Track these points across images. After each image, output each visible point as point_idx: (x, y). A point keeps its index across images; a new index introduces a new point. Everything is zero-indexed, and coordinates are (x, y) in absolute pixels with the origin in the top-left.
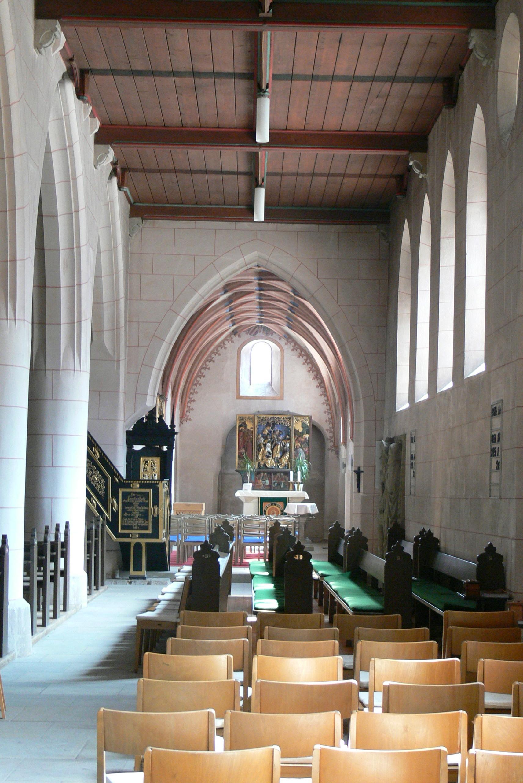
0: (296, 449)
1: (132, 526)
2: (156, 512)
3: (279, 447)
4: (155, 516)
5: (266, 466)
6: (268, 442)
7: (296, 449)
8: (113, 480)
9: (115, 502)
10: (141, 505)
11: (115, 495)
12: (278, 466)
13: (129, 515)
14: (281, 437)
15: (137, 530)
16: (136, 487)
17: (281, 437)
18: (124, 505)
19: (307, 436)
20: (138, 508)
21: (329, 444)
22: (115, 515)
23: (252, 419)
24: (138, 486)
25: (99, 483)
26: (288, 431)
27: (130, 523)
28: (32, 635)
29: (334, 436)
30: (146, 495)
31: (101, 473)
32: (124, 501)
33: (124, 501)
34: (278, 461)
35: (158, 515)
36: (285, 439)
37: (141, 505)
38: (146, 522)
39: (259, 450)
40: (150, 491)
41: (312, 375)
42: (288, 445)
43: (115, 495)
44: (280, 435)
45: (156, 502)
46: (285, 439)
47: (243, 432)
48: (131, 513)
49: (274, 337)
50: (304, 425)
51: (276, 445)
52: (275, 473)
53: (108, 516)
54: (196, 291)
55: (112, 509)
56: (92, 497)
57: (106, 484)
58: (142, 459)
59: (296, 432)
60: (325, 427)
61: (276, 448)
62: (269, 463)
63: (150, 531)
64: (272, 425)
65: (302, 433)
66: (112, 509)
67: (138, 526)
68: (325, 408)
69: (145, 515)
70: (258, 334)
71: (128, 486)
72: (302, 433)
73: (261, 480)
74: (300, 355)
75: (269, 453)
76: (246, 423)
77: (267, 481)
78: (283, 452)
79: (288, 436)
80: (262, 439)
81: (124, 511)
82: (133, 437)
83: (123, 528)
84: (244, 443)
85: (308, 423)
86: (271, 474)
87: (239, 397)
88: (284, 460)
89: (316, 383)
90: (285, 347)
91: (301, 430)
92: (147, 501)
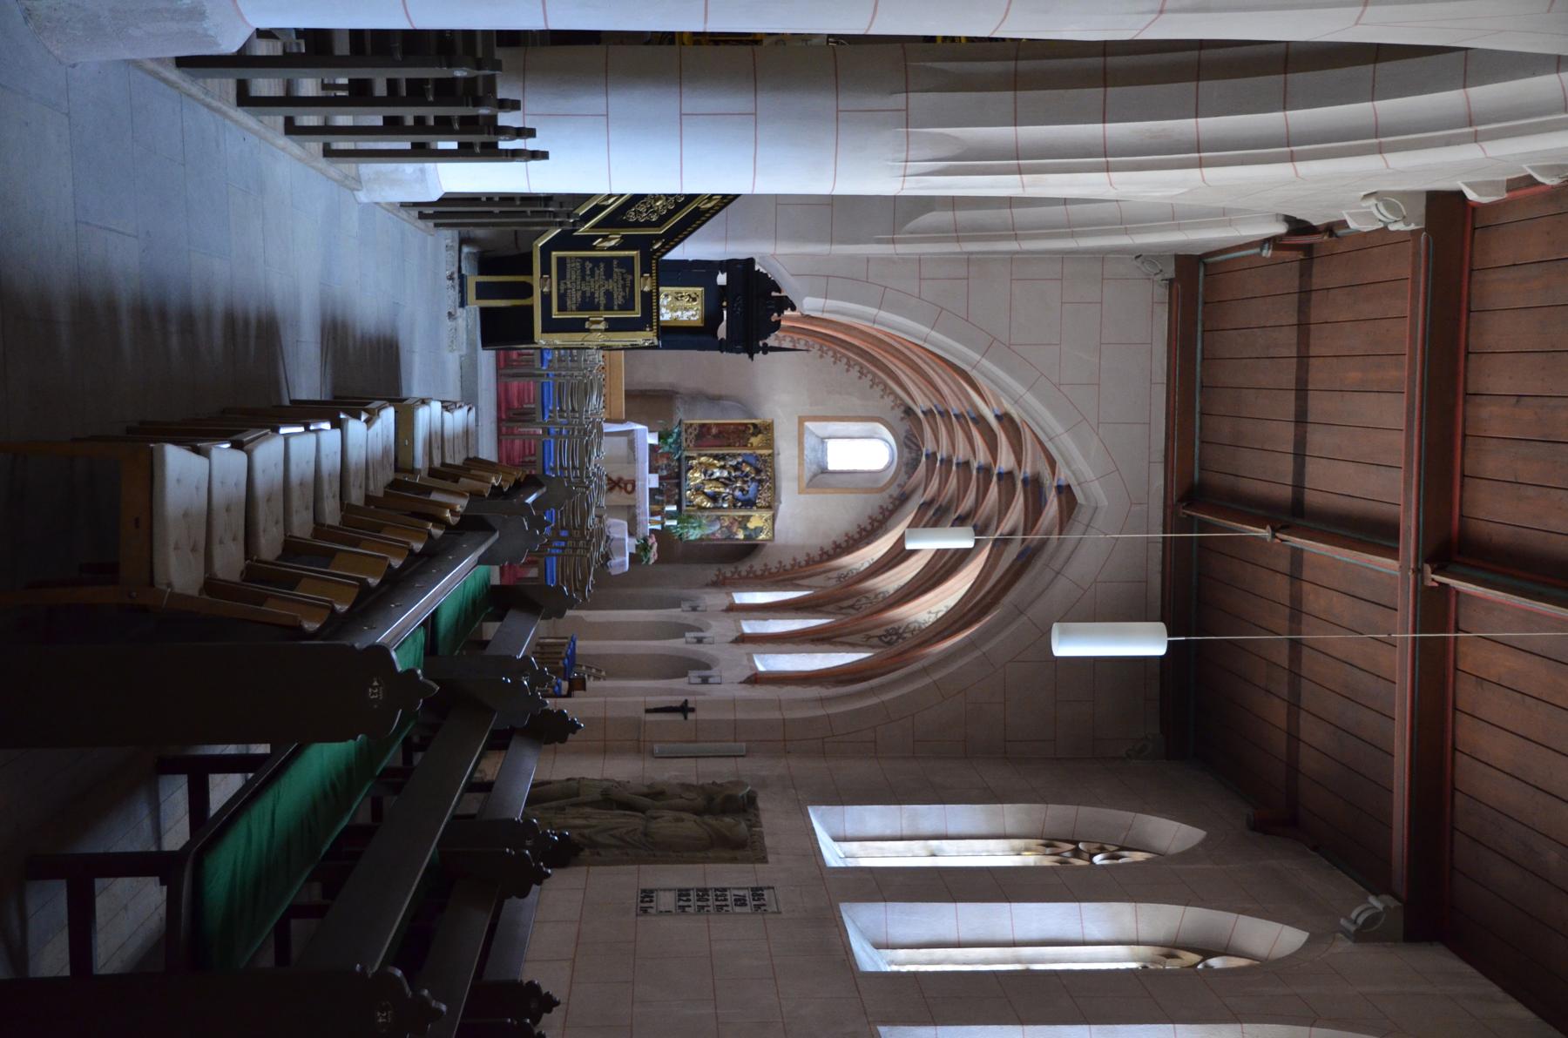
0: (718, 518)
7: (718, 518)
9: (613, 243)
10: (609, 294)
11: (626, 243)
14: (738, 493)
16: (644, 285)
17: (738, 493)
18: (608, 260)
19: (741, 535)
21: (728, 570)
22: (586, 243)
23: (769, 443)
24: (647, 289)
26: (749, 504)
27: (572, 275)
28: (183, 62)
29: (741, 578)
31: (671, 214)
34: (699, 490)
35: (588, 331)
36: (736, 499)
37: (609, 294)
39: (716, 457)
40: (637, 314)
41: (841, 540)
43: (626, 243)
44: (742, 490)
45: (614, 326)
49: (903, 477)
50: (758, 530)
51: (726, 485)
52: (679, 485)
53: (583, 230)
54: (1030, 389)
57: (648, 224)
58: (699, 290)
59: (748, 518)
60: (757, 564)
63: (556, 315)
65: (745, 528)
66: (597, 237)
68: (788, 563)
69: (588, 304)
70: (906, 450)
71: (646, 268)
72: (745, 528)
74: (872, 520)
78: (714, 497)
80: (734, 463)
82: (742, 270)
83: (561, 260)
85: (763, 536)
87: (802, 420)
89: (828, 546)
90: (885, 495)
91: (751, 525)
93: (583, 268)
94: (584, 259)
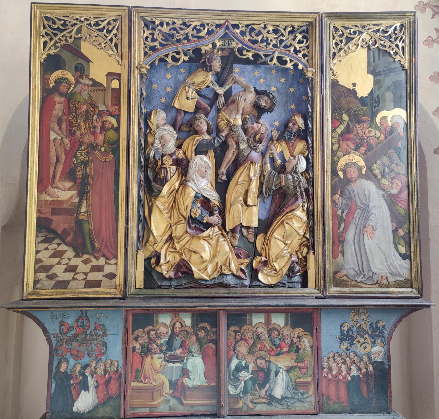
3: (254, 172)
5: (189, 273)
6: (200, 150)
7: (341, 184)
12: (254, 273)
14: (268, 124)
17: (268, 124)
34: (250, 244)
36: (285, 133)
42: (303, 165)
46: (285, 133)
47: (69, 98)
59: (343, 95)
61: (241, 176)
62: (207, 254)
64: (217, 65)
65: (373, 102)
72: (373, 102)
73: (157, 360)
75: (206, 203)
76: (86, 48)
77: (196, 364)
78: (279, 200)
79: (300, 121)
80: (170, 136)
84: (70, 153)
86: (215, 324)
88: (284, 242)
91: (364, 86)
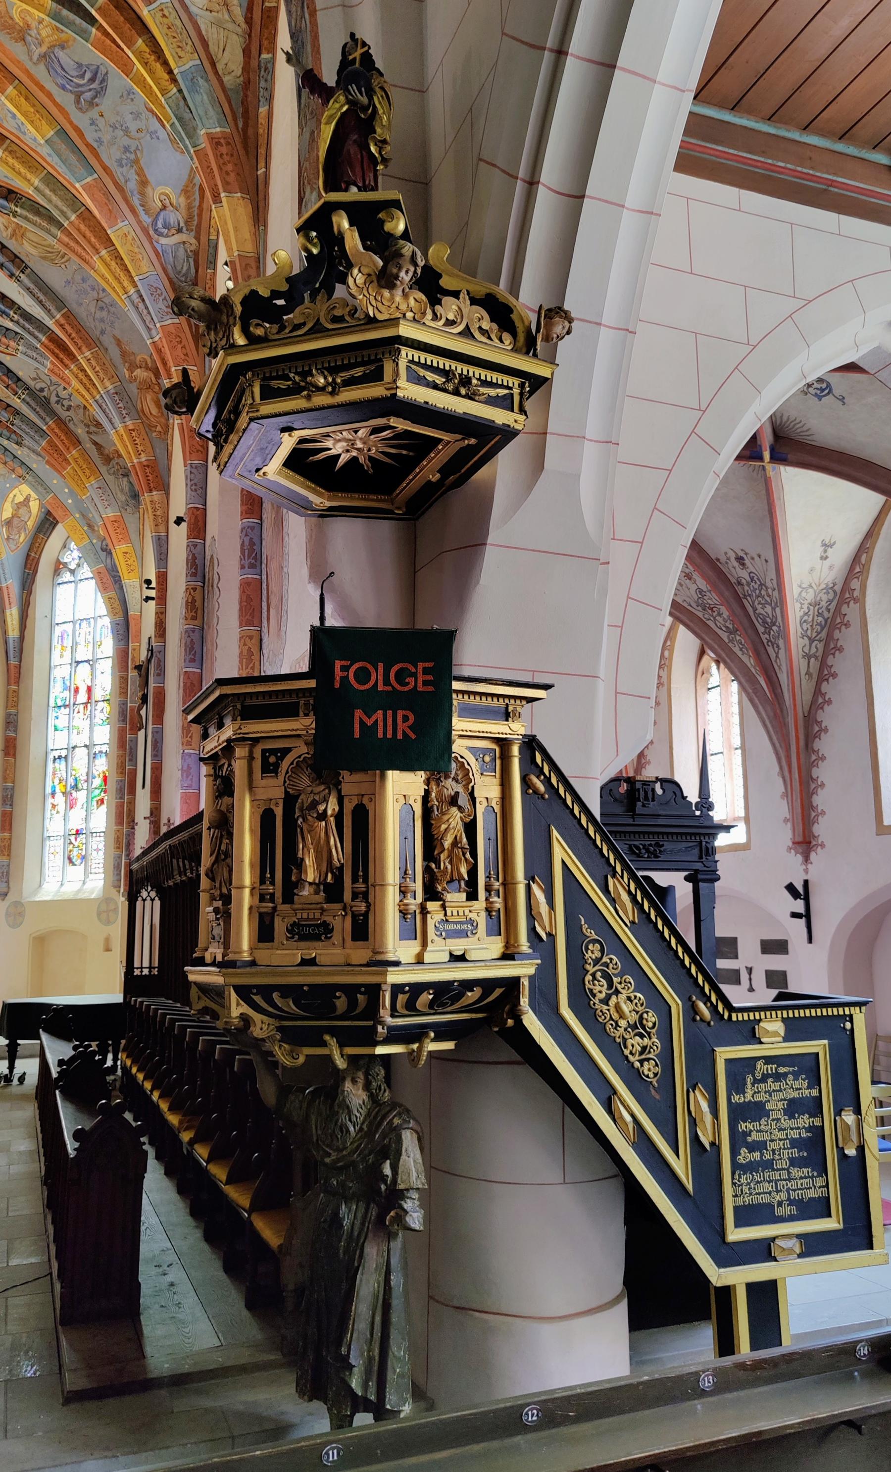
1: (770, 1206)
2: (854, 1137)
4: (851, 1152)
8: (691, 1011)
9: (704, 1105)
10: (793, 1108)
13: (757, 1155)
15: (791, 1218)
18: (738, 1113)
20: (786, 1123)
25: (639, 1027)
27: (760, 1190)
30: (808, 1067)
31: (645, 983)
32: (736, 1099)
33: (736, 1099)
35: (861, 1149)
37: (793, 1108)
38: (820, 1182)
40: (818, 1046)
43: (702, 1073)
45: (848, 1095)
48: (760, 1146)
53: (681, 1166)
55: (695, 1139)
56: (615, 1092)
63: (831, 1224)
67: (791, 1202)
69: (812, 1151)
81: (738, 1140)
92: (815, 1093)
93: (750, 1167)
94: (735, 1166)
